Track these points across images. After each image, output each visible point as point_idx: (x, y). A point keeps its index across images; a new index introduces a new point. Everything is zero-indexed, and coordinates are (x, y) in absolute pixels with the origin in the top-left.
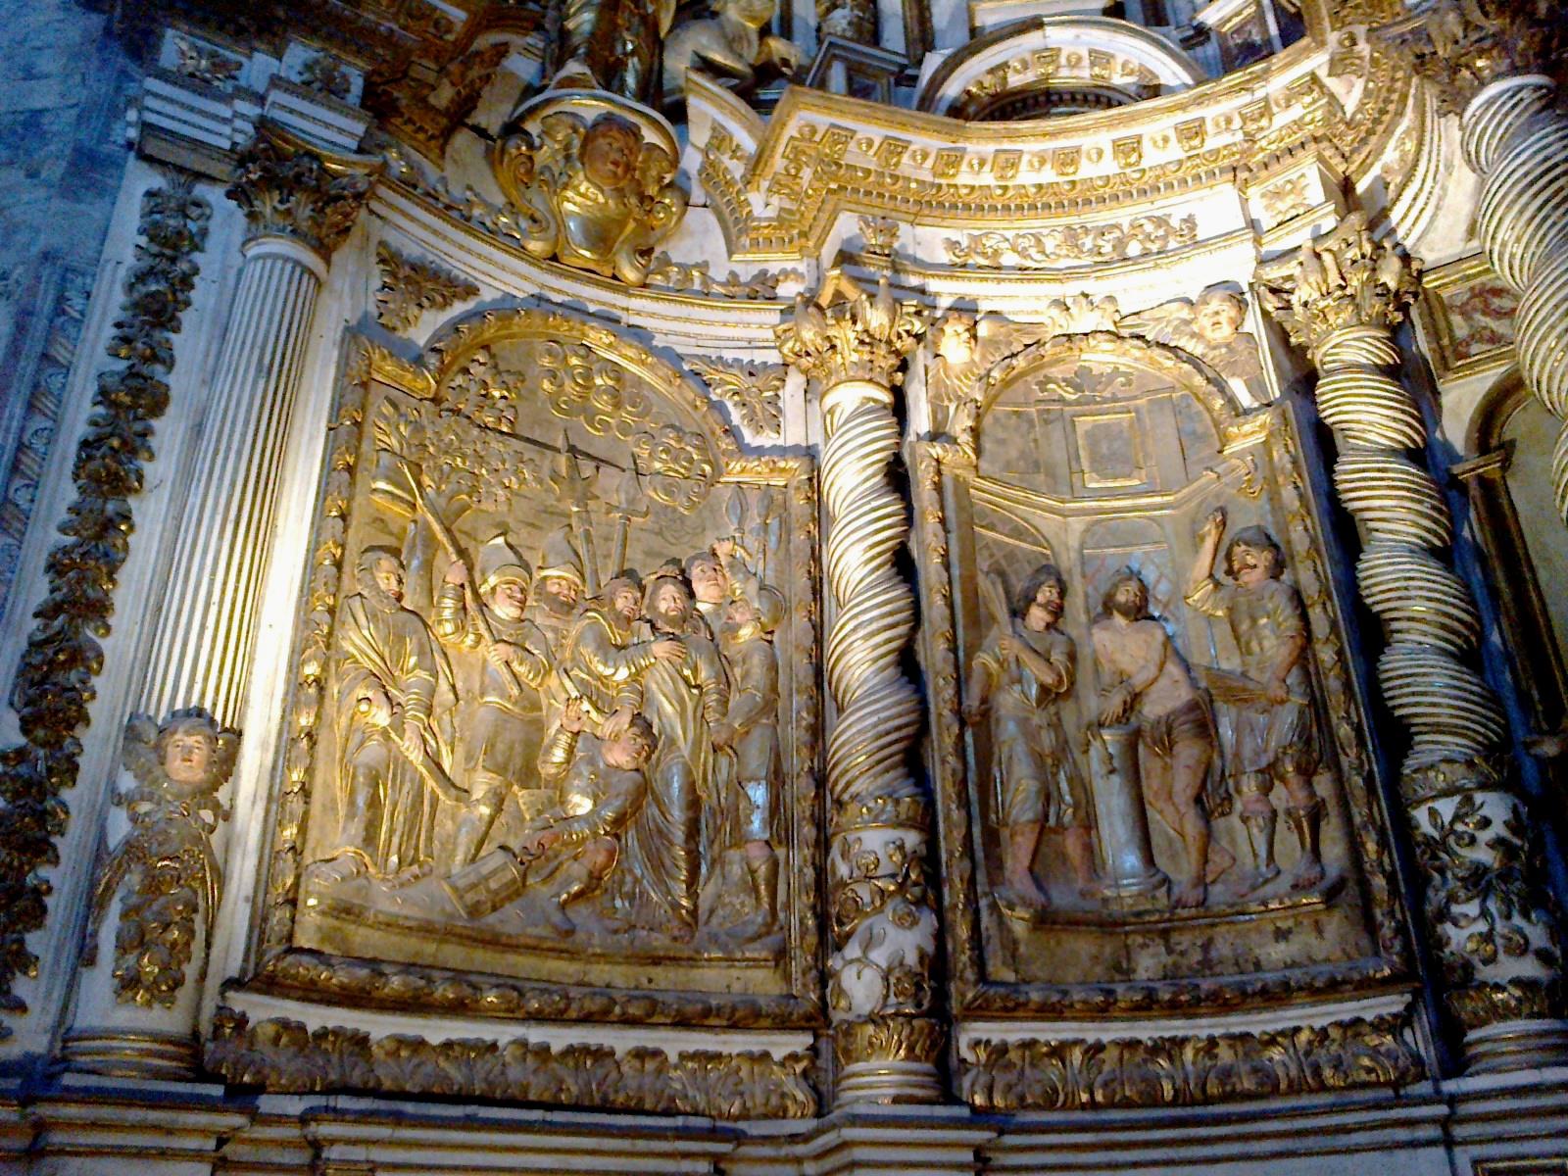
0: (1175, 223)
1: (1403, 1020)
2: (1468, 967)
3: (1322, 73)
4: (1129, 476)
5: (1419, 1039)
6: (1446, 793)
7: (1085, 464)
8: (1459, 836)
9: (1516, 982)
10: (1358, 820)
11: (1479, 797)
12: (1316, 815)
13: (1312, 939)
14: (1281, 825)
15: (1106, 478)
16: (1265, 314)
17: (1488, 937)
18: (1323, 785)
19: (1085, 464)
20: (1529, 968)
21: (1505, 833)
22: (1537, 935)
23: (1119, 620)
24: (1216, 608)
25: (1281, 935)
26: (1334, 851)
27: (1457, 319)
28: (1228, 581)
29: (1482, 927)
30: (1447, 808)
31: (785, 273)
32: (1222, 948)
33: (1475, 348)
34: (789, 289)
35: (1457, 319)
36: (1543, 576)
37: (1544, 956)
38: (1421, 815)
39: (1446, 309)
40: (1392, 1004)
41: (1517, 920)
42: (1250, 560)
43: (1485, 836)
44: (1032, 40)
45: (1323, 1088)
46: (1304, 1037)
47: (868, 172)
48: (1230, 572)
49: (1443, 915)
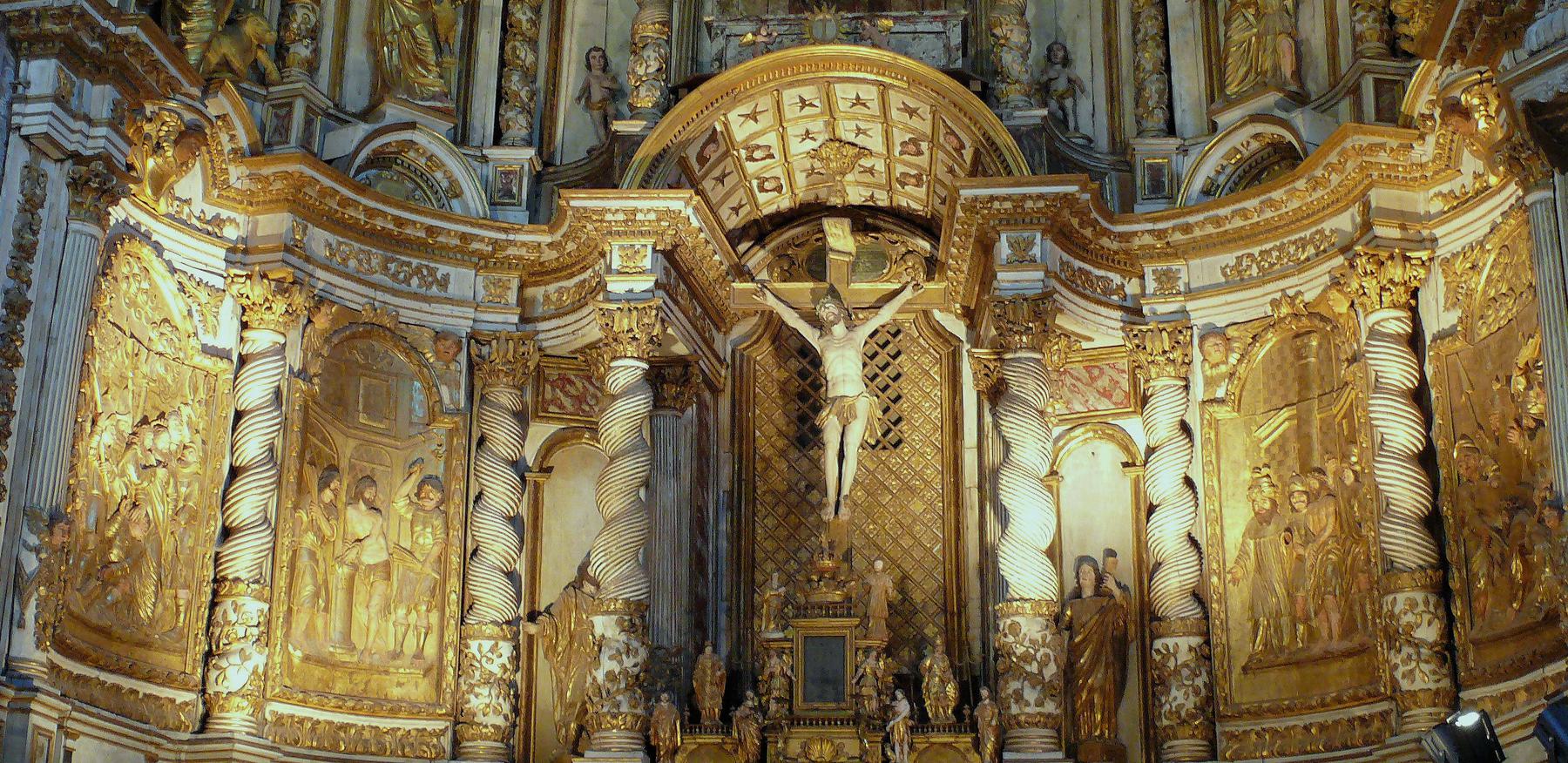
0: (439, 276)
1: (443, 732)
2: (474, 715)
3: (543, 246)
4: (381, 422)
5: (446, 742)
6: (490, 638)
7: (361, 407)
8: (489, 659)
9: (494, 726)
10: (446, 639)
11: (501, 643)
12: (428, 629)
13: (413, 690)
14: (410, 633)
15: (369, 419)
16: (469, 354)
17: (488, 706)
18: (434, 618)
19: (361, 407)
20: (500, 721)
21: (506, 662)
22: (506, 708)
23: (362, 506)
24: (407, 512)
25: (400, 684)
26: (431, 650)
27: (548, 387)
28: (415, 499)
29: (487, 701)
30: (487, 645)
31: (231, 220)
32: (373, 685)
33: (552, 408)
34: (231, 232)
35: (548, 387)
36: (544, 540)
37: (506, 717)
38: (473, 645)
39: (546, 380)
40: (439, 725)
41: (501, 700)
42: (431, 496)
43: (498, 661)
44: (406, 135)
45: (404, 756)
46: (399, 733)
47: (311, 197)
48: (418, 495)
49: (471, 691)
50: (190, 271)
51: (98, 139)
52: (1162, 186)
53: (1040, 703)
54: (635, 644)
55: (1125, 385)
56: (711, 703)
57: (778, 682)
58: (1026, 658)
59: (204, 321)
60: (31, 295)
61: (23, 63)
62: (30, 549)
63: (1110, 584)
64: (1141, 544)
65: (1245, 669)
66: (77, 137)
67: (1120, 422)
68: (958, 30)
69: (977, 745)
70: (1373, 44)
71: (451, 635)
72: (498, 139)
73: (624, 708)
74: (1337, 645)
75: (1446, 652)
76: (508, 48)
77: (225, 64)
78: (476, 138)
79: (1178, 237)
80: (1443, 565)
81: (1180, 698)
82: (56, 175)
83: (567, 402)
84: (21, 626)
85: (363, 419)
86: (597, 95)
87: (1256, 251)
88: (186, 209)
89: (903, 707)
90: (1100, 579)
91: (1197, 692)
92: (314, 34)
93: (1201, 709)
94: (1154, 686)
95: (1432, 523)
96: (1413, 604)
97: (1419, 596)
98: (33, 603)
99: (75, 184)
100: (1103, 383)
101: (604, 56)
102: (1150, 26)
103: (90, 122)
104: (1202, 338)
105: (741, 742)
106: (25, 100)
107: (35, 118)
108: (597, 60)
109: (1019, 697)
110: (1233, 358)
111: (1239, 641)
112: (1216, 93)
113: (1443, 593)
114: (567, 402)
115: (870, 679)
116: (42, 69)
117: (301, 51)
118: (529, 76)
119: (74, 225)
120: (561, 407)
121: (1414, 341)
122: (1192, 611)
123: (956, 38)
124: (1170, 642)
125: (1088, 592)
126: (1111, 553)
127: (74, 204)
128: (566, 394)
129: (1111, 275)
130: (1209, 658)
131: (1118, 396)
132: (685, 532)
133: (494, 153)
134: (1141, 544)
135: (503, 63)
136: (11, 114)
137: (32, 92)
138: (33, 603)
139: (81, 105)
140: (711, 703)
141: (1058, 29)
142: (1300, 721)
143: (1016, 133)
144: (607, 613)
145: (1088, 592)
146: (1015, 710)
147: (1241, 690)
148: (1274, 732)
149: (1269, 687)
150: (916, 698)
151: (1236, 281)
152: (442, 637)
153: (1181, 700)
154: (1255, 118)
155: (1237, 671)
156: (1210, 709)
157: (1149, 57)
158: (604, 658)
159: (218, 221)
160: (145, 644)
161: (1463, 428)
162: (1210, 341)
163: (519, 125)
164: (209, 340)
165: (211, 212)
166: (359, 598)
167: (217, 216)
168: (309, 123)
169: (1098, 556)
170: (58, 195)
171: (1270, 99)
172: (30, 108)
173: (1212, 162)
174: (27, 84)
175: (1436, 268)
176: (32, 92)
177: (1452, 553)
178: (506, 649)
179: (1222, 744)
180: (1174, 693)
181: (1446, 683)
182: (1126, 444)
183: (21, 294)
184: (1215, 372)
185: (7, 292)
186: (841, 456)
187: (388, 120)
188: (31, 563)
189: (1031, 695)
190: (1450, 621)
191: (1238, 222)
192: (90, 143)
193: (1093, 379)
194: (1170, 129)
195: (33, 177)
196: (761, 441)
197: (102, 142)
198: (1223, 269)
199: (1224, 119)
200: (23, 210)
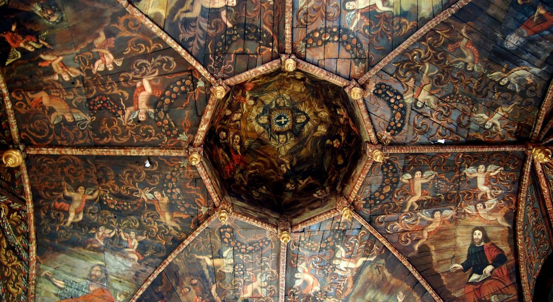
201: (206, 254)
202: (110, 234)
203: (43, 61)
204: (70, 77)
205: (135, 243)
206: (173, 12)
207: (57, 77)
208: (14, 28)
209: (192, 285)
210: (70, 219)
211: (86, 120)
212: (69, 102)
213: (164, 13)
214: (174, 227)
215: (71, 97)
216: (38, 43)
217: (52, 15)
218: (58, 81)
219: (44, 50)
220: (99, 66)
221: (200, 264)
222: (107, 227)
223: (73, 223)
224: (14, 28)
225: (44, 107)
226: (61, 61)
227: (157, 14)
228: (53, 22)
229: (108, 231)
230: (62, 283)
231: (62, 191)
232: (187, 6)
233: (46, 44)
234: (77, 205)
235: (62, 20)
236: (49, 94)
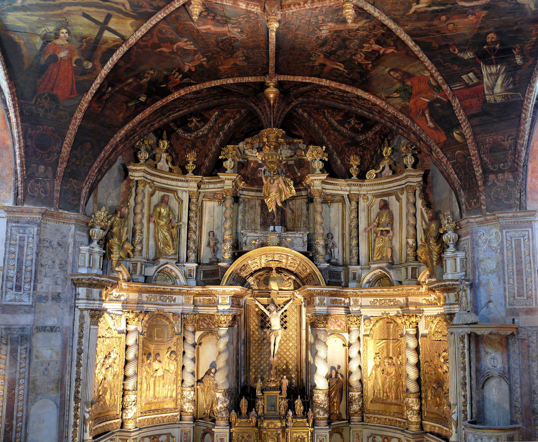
5: (178, 417)
18: (175, 386)
20: (191, 411)
22: (193, 408)
23: (157, 361)
26: (174, 395)
30: (188, 393)
31: (123, 295)
32: (161, 406)
33: (201, 327)
34: (122, 298)
38: (185, 393)
50: (113, 312)
51: (96, 305)
52: (356, 278)
53: (324, 415)
54: (226, 399)
55: (344, 324)
56: (244, 410)
57: (261, 407)
58: (321, 404)
59: (118, 324)
60: (83, 348)
61: (77, 289)
62: (87, 413)
63: (339, 376)
64: (347, 366)
65: (371, 402)
66: (91, 305)
67: (343, 334)
68: (306, 236)
69: (308, 421)
70: (411, 258)
71: (179, 390)
72: (187, 261)
73: (224, 416)
74: (394, 401)
75: (420, 412)
76: (189, 234)
77: (121, 257)
78: (181, 260)
79: (359, 293)
80: (420, 391)
81: (355, 407)
82: (86, 313)
83: (205, 325)
84: (86, 432)
85: (156, 339)
86: (212, 244)
87: (379, 299)
88: (112, 296)
89: (290, 413)
90: (337, 373)
91: (359, 406)
92: (141, 242)
93: (360, 409)
94: (349, 402)
95: (418, 381)
96: (413, 402)
97: (414, 400)
98: (88, 425)
99: (92, 317)
100: (338, 323)
101: (214, 234)
102: (354, 234)
103: (94, 300)
104: (364, 320)
105: (251, 421)
106: (79, 299)
107: (82, 304)
108: (211, 233)
109: (318, 412)
110: (371, 325)
111: (369, 393)
112: (370, 259)
113: (420, 398)
114: (205, 325)
115: (282, 406)
116: (83, 290)
117: (138, 248)
118: (194, 242)
119: (92, 327)
120: (204, 326)
121: (417, 336)
122: (359, 386)
123: (306, 239)
124: (354, 393)
125: (334, 376)
126: (339, 367)
127: (91, 321)
128: (205, 323)
129: (342, 298)
130: (362, 397)
131: (342, 327)
132: (235, 355)
133: (186, 265)
134: (347, 366)
135: (188, 238)
136: (75, 303)
137: (80, 297)
138: (88, 425)
139: (91, 296)
140: (244, 410)
141: (330, 227)
142: (385, 417)
143: (320, 270)
144: (220, 392)
145: (334, 376)
146: (317, 416)
147: (369, 406)
148: (378, 418)
149: (377, 407)
150: (294, 410)
151: (373, 306)
152: (177, 391)
153: (356, 408)
154: (380, 268)
155: (369, 402)
156: (362, 410)
157: (354, 242)
158: (219, 404)
159: (119, 296)
160: (108, 411)
161: (427, 359)
162: (366, 321)
163: (193, 256)
164: (119, 329)
165: (117, 294)
166: (157, 385)
167: (119, 296)
168: (141, 267)
169: (336, 367)
170: (88, 319)
171: (384, 265)
172: (80, 301)
173: (367, 277)
174: (79, 294)
175: (423, 318)
176: (80, 297)
177: (423, 388)
178: (192, 393)
179: (365, 419)
180: (354, 406)
181: (419, 420)
182: (344, 339)
183: (80, 348)
184: (367, 328)
185: (77, 350)
186: (275, 345)
187: (161, 263)
188: (87, 416)
189: (321, 413)
190: (421, 405)
191: (374, 293)
192: (95, 305)
193: (336, 322)
194: (358, 263)
195: (82, 317)
196: (252, 327)
197: (98, 305)
198: (370, 302)
199: (373, 266)
200: (79, 327)
201: (411, 7)
202: (362, 56)
203: (190, 70)
204: (203, 58)
205: (376, 47)
206: (127, 15)
207: (204, 63)
208: (163, 86)
209: (446, 21)
210: (341, 69)
211: (243, 52)
212: (225, 59)
213: (130, 21)
214: (365, 23)
215: (222, 58)
216: (175, 74)
217: (149, 73)
218: (207, 63)
219: (180, 71)
220: (191, 47)
221: (421, 12)
222: (355, 55)
223: (345, 69)
224: (163, 86)
225: (232, 68)
226: (189, 63)
227: (132, 25)
228: (154, 72)
229: (358, 55)
230: (395, 94)
231: (313, 67)
232: (120, 7)
233: (175, 71)
234: (328, 63)
235: (151, 69)
236: (220, 65)
